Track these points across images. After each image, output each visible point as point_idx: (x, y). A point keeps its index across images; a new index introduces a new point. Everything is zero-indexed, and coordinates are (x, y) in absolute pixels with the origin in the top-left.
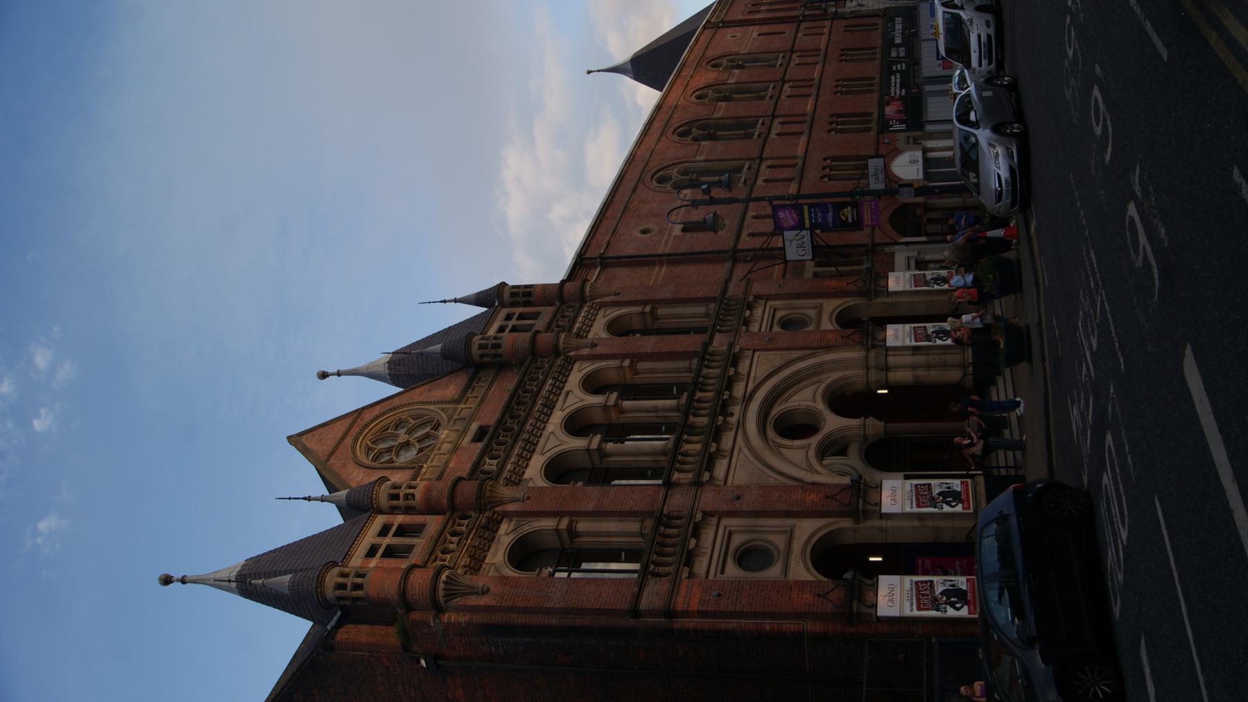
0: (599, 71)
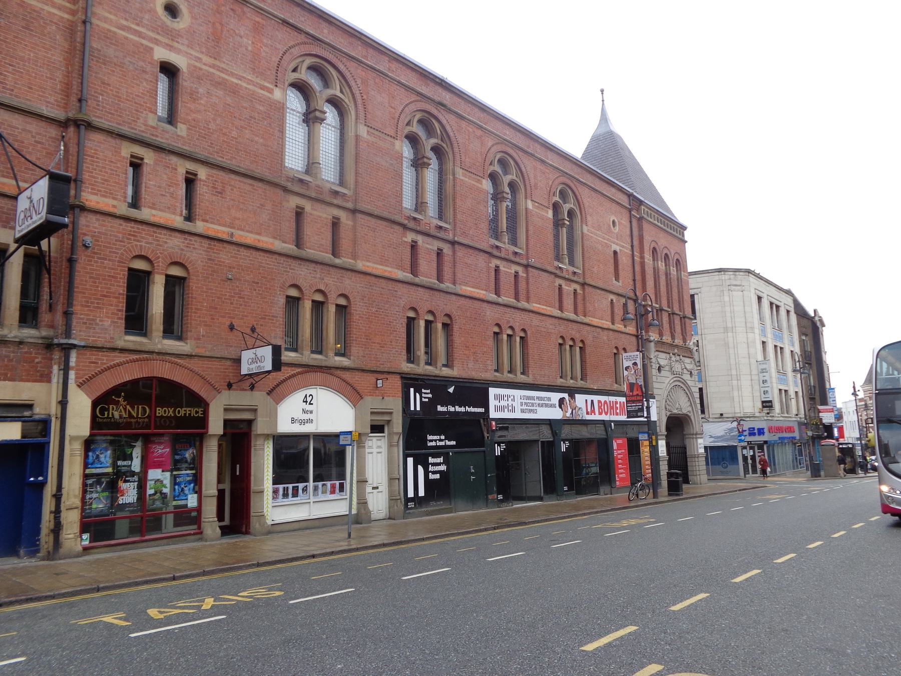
0: (603, 101)
